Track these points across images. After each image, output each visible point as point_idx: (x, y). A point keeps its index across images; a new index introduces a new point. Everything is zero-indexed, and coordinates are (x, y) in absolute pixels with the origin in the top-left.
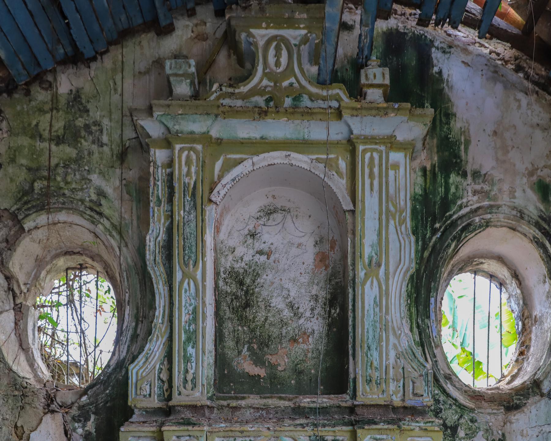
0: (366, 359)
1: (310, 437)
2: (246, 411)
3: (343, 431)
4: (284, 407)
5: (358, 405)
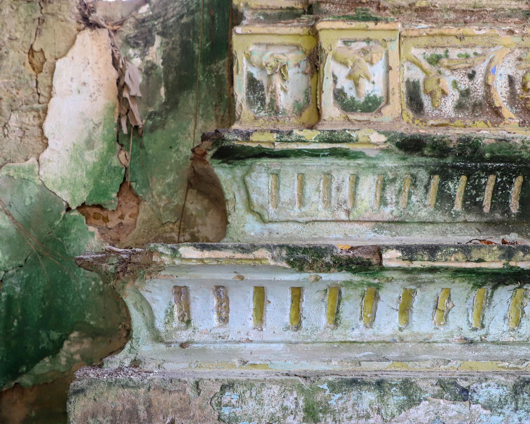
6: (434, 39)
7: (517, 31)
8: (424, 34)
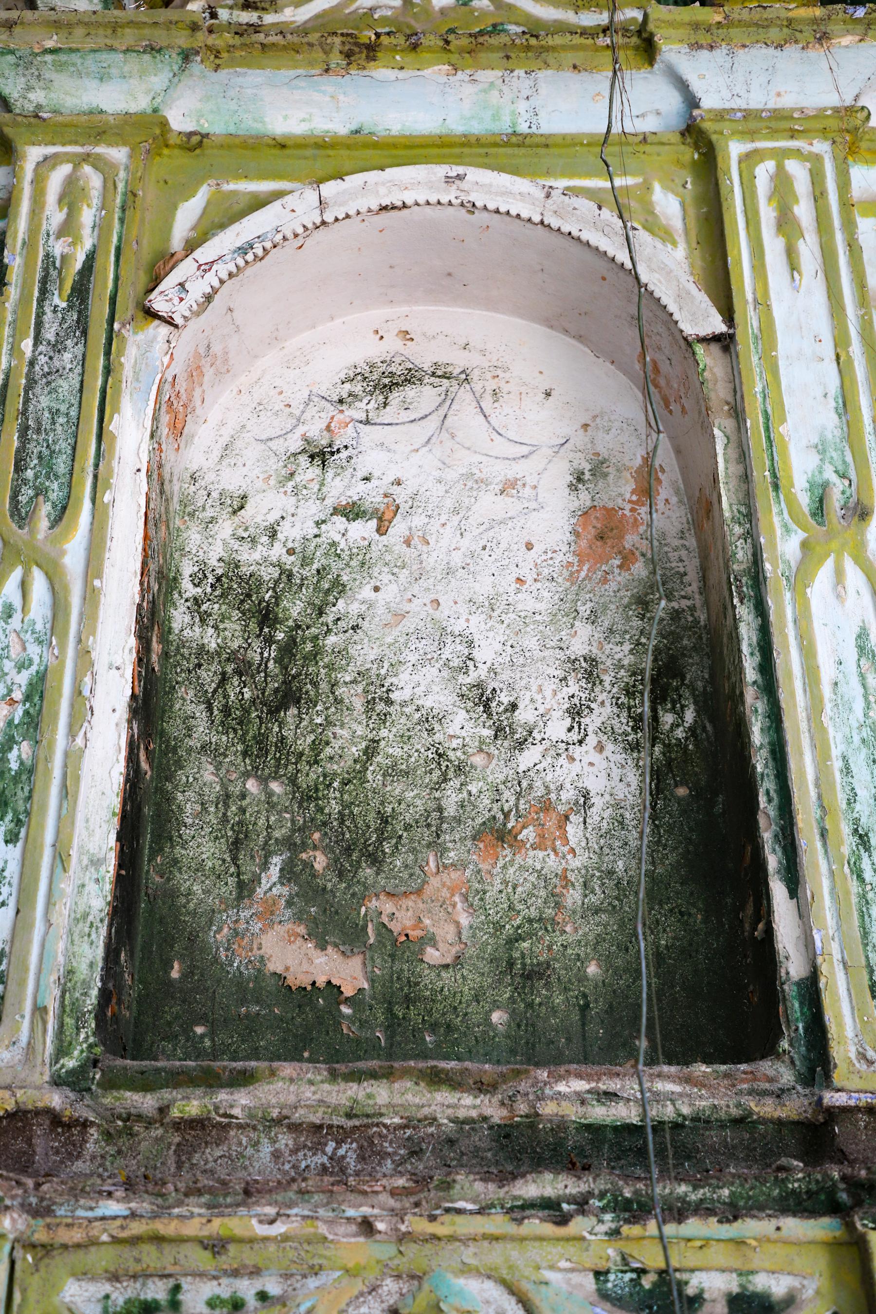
0: (854, 886)
1: (600, 1274)
2: (256, 1144)
3: (786, 1242)
4: (454, 1120)
5: (846, 1110)
6: (135, 1253)
7: (380, 1226)
8: (105, 1238)
